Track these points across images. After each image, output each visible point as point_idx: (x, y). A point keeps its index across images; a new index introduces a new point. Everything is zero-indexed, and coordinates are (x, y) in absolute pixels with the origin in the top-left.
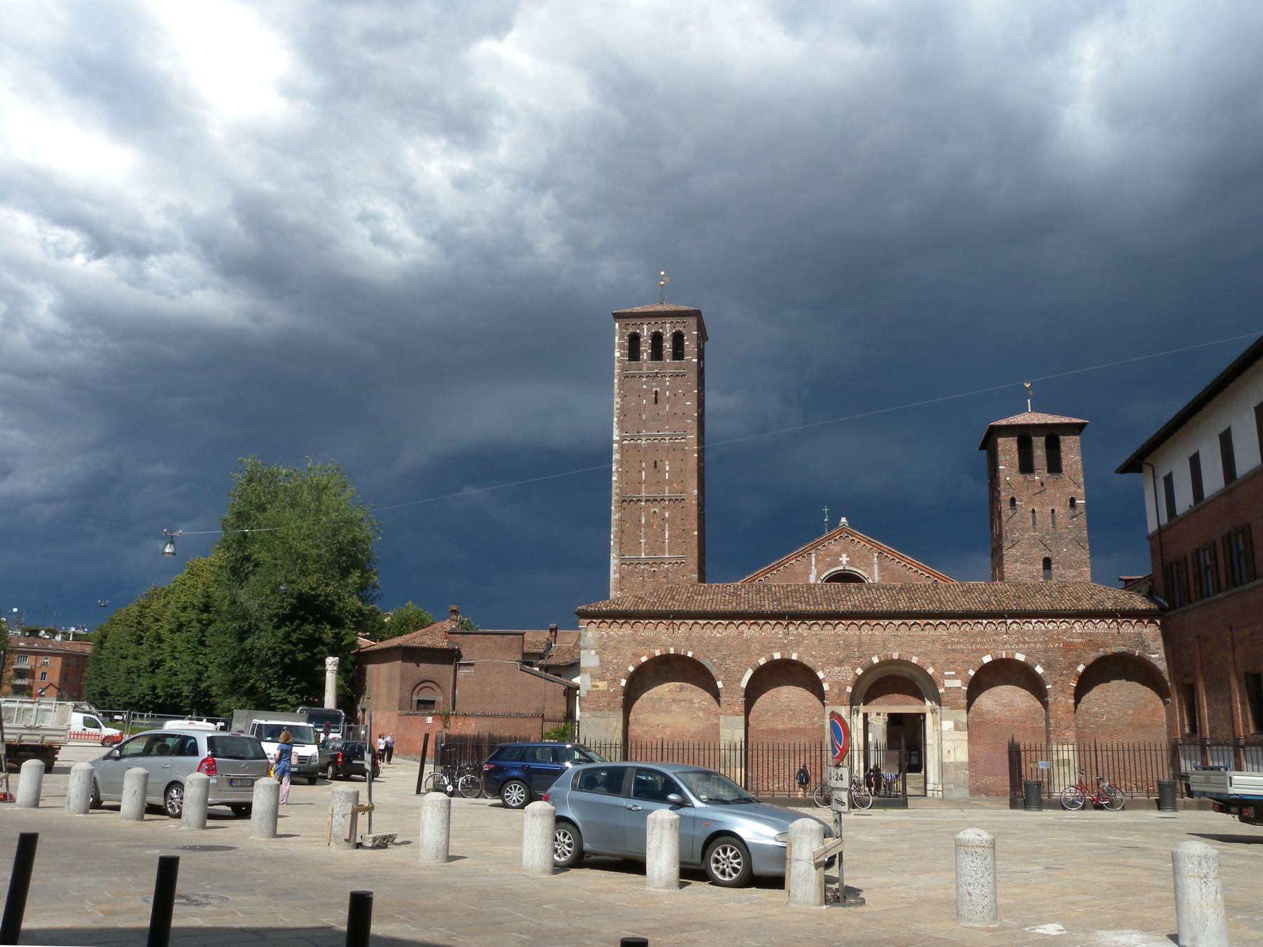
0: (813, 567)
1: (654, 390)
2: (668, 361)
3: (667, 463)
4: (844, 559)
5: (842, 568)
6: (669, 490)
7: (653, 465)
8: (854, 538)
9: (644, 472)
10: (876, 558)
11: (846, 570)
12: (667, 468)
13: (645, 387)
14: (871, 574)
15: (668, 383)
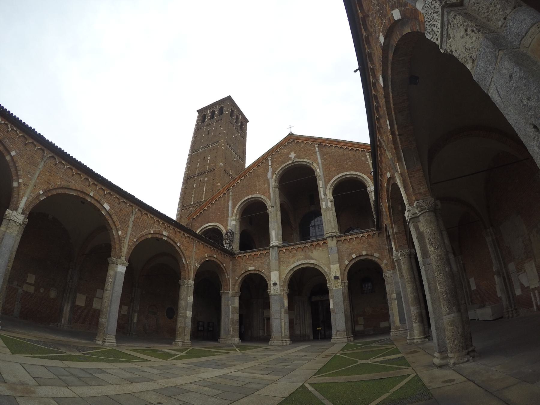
0: (270, 167)
1: (208, 130)
2: (216, 117)
3: (209, 155)
4: (293, 155)
5: (291, 162)
6: (208, 167)
7: (203, 157)
8: (298, 141)
9: (198, 164)
10: (317, 148)
11: (296, 162)
12: (209, 158)
13: (205, 130)
14: (316, 160)
15: (214, 125)
